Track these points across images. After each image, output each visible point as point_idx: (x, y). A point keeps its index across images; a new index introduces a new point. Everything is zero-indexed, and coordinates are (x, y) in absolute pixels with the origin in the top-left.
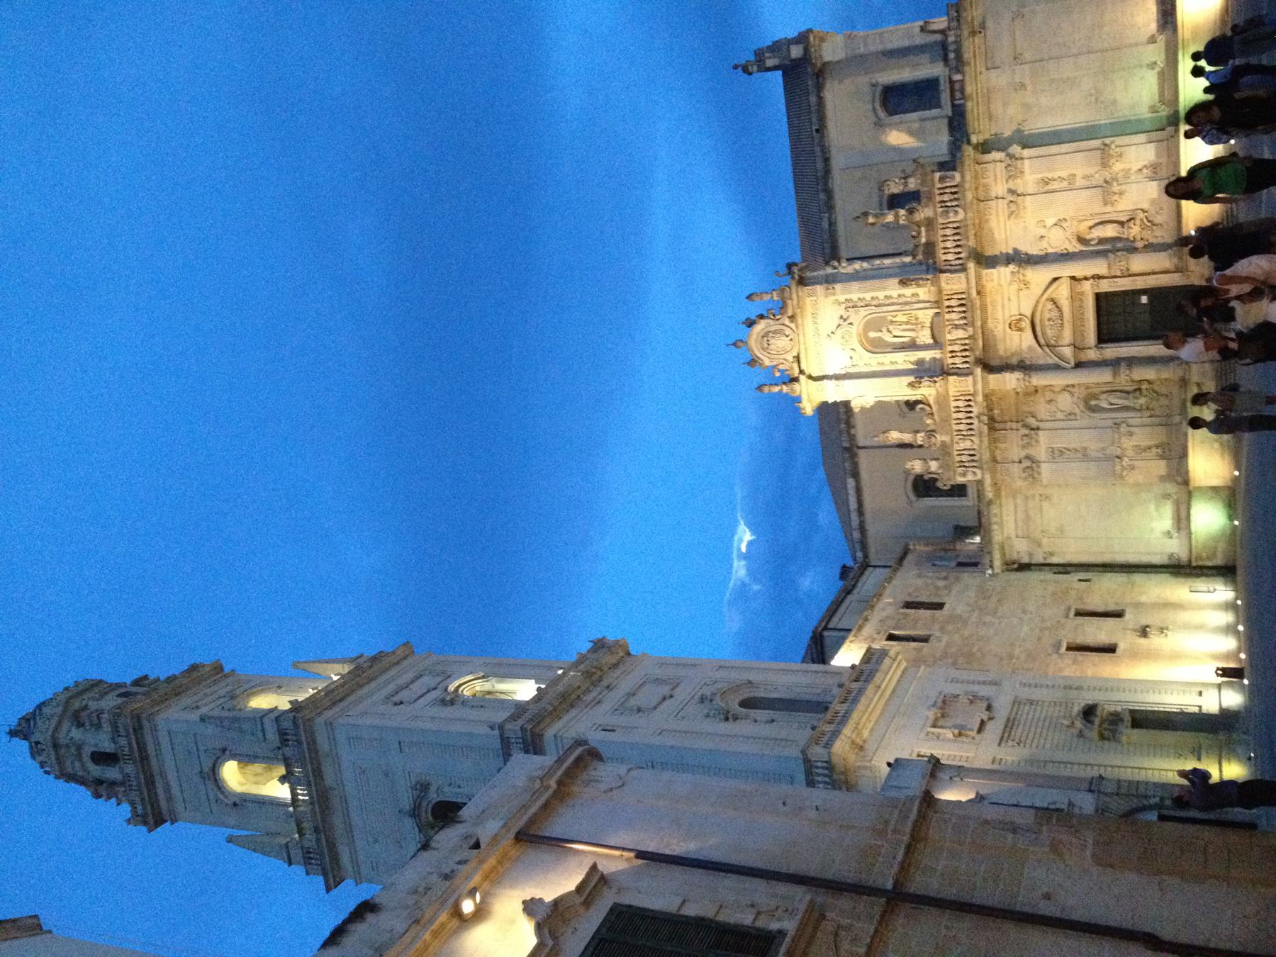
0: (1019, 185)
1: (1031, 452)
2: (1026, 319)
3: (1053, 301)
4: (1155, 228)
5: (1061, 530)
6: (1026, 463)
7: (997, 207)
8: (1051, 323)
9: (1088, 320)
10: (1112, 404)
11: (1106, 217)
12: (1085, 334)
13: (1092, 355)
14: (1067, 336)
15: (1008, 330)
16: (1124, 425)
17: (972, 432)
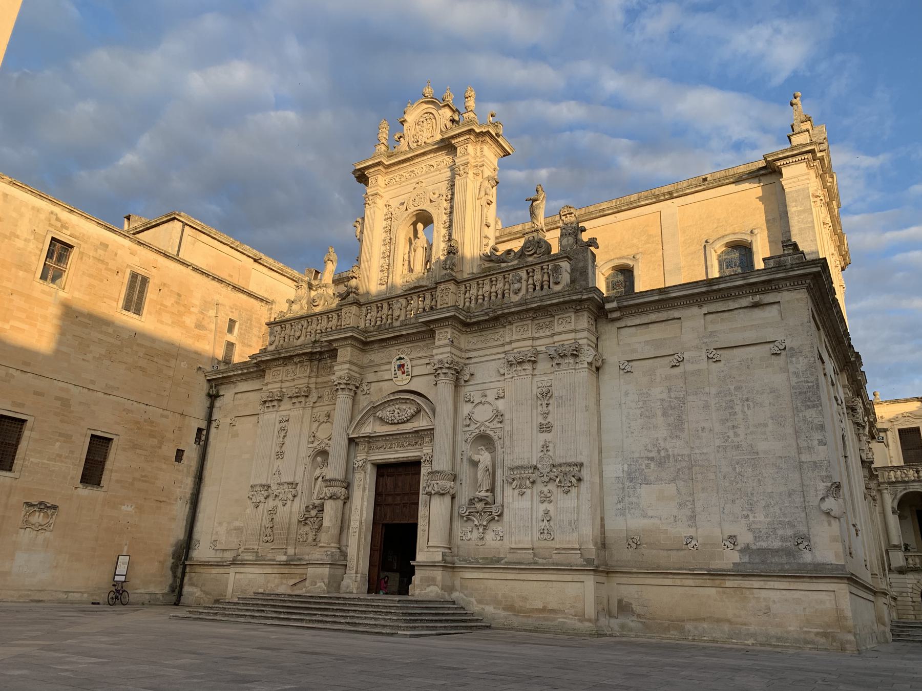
1: (286, 400)
3: (418, 412)
4: (481, 530)
5: (235, 435)
11: (499, 472)
12: (382, 450)
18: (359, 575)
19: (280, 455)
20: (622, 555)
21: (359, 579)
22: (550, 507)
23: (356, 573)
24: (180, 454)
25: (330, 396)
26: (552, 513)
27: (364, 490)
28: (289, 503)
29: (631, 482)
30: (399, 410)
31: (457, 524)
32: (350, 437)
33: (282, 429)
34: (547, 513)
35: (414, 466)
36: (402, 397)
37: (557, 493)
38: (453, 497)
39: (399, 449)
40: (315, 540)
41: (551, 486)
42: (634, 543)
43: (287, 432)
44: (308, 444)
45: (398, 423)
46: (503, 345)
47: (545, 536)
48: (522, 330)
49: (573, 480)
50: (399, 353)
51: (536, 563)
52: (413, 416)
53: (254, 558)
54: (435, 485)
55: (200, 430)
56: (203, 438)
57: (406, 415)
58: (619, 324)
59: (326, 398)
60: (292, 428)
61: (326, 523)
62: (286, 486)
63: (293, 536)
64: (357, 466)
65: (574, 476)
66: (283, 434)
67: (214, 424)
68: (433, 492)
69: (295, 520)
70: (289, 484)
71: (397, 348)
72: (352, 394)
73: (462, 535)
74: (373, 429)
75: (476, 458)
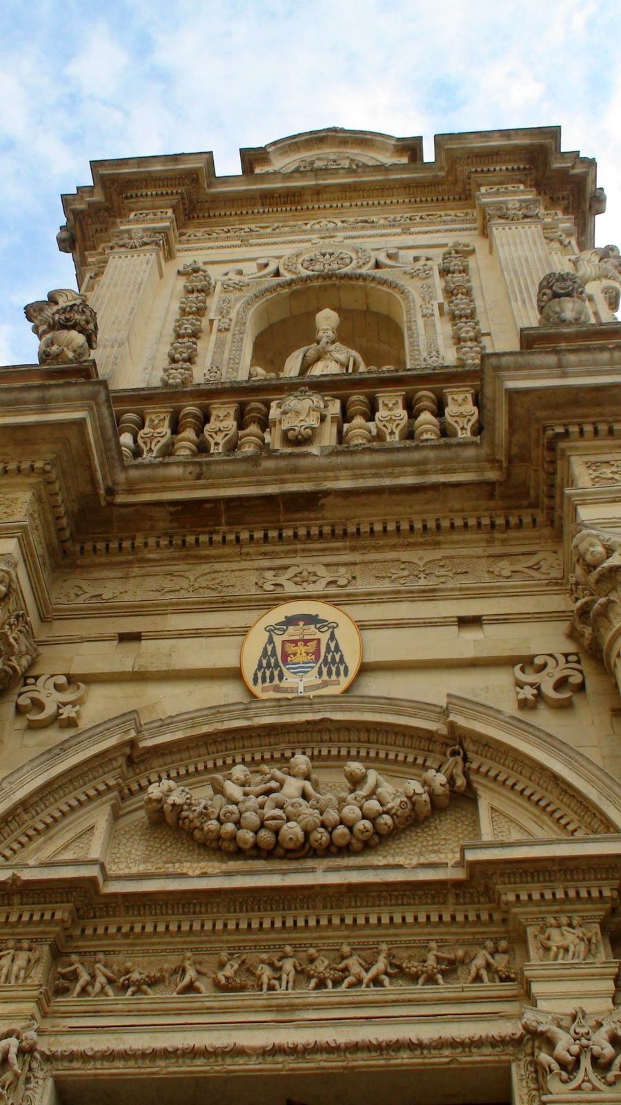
9: (285, 1012)
30: (308, 785)
39: (314, 997)
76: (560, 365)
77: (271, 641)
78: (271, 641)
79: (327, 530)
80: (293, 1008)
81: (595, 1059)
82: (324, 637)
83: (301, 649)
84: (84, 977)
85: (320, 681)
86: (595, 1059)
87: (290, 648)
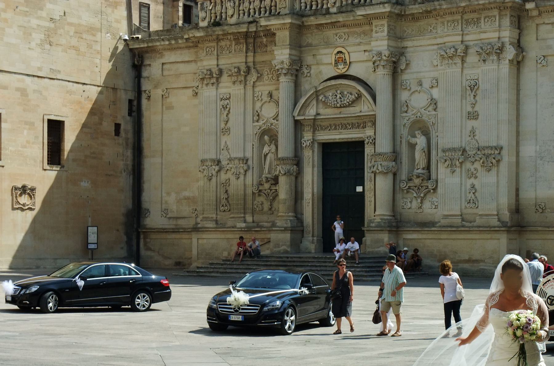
0: (472, 58)
1: (225, 78)
2: (346, 69)
3: (359, 96)
4: (419, 200)
5: (170, 108)
6: (215, 70)
7: (456, 35)
8: (339, 96)
10: (266, 156)
11: (433, 153)
13: (307, 136)
14: (327, 113)
15: (336, 51)
16: (245, 168)
17: (241, 15)
18: (315, 238)
19: (226, 131)
20: (531, 216)
21: (315, 241)
22: (476, 182)
23: (313, 236)
24: (117, 127)
25: (270, 76)
26: (476, 187)
27: (313, 167)
28: (242, 177)
29: (541, 160)
31: (399, 196)
32: (295, 119)
33: (225, 107)
34: (473, 186)
35: (359, 146)
36: (343, 83)
37: (481, 173)
38: (395, 174)
40: (270, 209)
41: (477, 165)
42: (541, 208)
43: (229, 111)
44: (253, 123)
45: (341, 107)
46: (435, 38)
47: (472, 205)
48: (453, 25)
49: (494, 161)
50: (337, 38)
51: (463, 226)
52: (353, 102)
53: (215, 226)
54: (379, 166)
55: (130, 101)
56: (134, 108)
57: (348, 101)
58: (539, 21)
59: (266, 77)
60: (236, 108)
61: (282, 195)
62: (236, 161)
63: (249, 205)
64: (304, 145)
65: (494, 158)
66: (226, 112)
67: (144, 96)
68: (377, 171)
69: (249, 191)
70: (240, 159)
71: (334, 32)
72: (294, 78)
73: (403, 205)
74: (317, 111)
75: (413, 141)
76: (365, 9)
77: (336, 57)
78: (336, 57)
79: (342, 25)
80: (342, 132)
81: (370, 142)
82: (343, 56)
83: (340, 59)
84: (318, 128)
85: (343, 67)
86: (370, 142)
87: (339, 59)
